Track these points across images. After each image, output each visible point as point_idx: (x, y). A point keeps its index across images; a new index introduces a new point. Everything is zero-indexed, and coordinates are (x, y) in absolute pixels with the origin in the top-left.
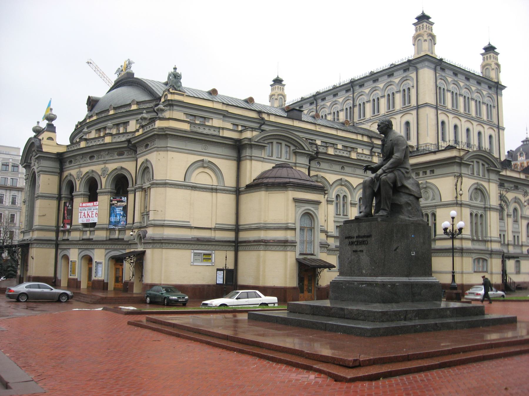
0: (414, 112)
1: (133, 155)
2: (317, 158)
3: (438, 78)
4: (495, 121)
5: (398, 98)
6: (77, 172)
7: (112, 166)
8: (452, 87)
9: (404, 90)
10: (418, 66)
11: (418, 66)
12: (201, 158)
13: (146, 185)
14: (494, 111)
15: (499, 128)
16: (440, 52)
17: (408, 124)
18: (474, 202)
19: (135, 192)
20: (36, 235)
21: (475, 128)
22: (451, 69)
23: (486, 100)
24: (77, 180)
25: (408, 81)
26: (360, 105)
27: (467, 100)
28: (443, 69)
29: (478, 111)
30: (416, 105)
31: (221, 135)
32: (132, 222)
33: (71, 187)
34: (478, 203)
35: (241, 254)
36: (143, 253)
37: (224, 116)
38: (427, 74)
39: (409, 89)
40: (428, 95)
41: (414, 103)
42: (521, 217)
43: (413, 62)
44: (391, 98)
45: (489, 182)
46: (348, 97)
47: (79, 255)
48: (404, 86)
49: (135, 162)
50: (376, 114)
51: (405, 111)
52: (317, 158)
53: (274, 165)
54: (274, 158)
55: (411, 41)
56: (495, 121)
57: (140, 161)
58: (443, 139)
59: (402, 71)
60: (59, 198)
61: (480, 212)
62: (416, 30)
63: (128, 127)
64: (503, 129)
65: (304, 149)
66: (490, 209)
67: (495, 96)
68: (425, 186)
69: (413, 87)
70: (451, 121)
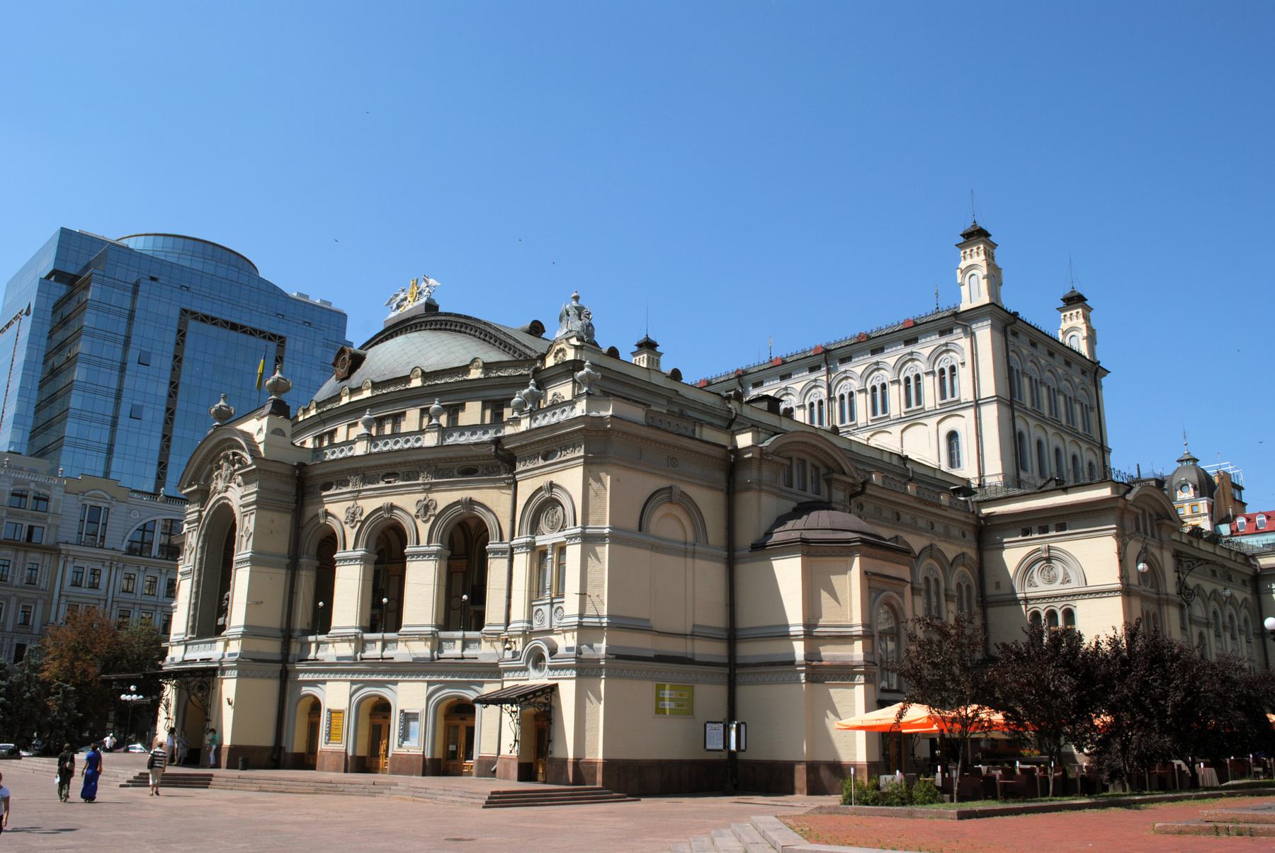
0: (970, 413)
2: (862, 492)
4: (1096, 436)
5: (930, 387)
7: (443, 499)
9: (942, 371)
12: (664, 483)
13: (546, 539)
14: (1093, 416)
15: (1104, 450)
17: (952, 436)
18: (1143, 587)
19: (511, 554)
21: (1070, 448)
24: (347, 527)
26: (842, 397)
27: (1053, 393)
28: (1015, 334)
30: (971, 399)
31: (697, 436)
32: (503, 621)
33: (329, 542)
34: (1148, 590)
35: (743, 692)
36: (553, 689)
37: (670, 400)
39: (953, 369)
41: (965, 393)
42: (1190, 620)
43: (965, 316)
44: (912, 388)
45: (1161, 548)
46: (815, 380)
47: (351, 696)
48: (944, 363)
50: (880, 415)
52: (862, 492)
53: (794, 504)
54: (795, 488)
56: (1096, 436)
57: (526, 488)
58: (1025, 470)
60: (293, 567)
61: (1153, 608)
63: (461, 415)
64: (1109, 451)
65: (844, 473)
66: (1168, 602)
68: (1045, 555)
69: (963, 364)
70: (1033, 432)
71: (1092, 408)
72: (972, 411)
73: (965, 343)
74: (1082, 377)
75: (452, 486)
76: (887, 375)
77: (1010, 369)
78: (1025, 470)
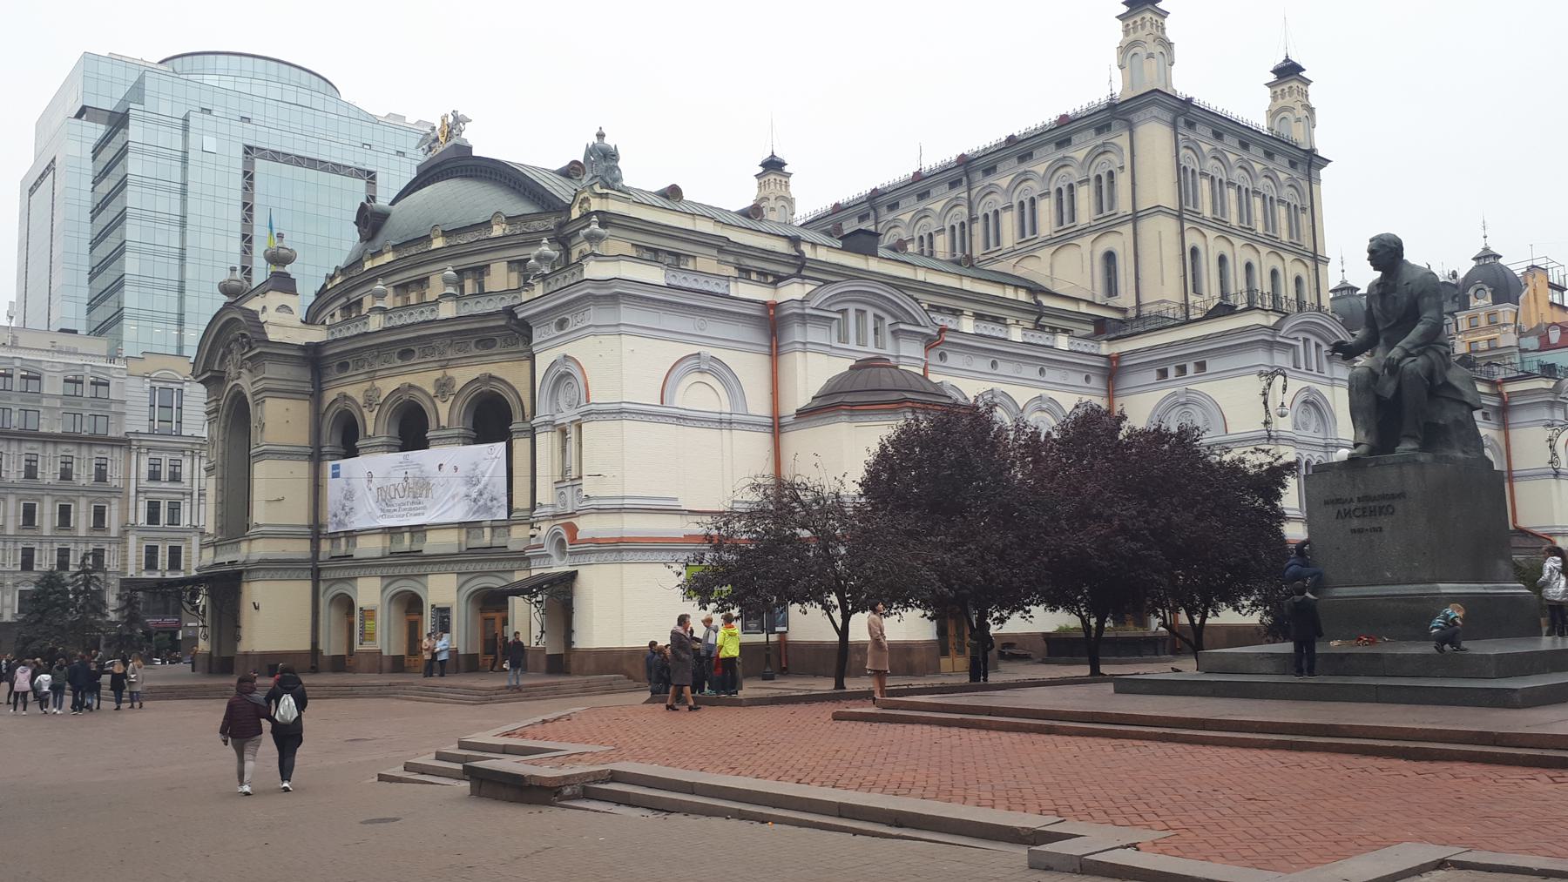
0: (1127, 229)
1: (521, 347)
3: (1181, 145)
6: (368, 391)
8: (1210, 165)
9: (1099, 178)
10: (1134, 117)
11: (1134, 117)
16: (1183, 83)
17: (1110, 257)
20: (257, 550)
22: (1208, 124)
23: (1287, 193)
25: (1109, 156)
29: (1270, 219)
38: (1155, 137)
39: (1111, 174)
40: (1159, 188)
48: (1100, 168)
49: (527, 363)
51: (1104, 226)
55: (1113, 58)
57: (543, 361)
58: (1196, 291)
59: (1092, 131)
62: (1126, 32)
67: (1305, 185)
69: (1122, 168)
71: (1303, 209)
72: (1130, 226)
73: (1123, 140)
74: (1290, 171)
75: (469, 361)
76: (1035, 187)
77: (1181, 170)
78: (1196, 291)
